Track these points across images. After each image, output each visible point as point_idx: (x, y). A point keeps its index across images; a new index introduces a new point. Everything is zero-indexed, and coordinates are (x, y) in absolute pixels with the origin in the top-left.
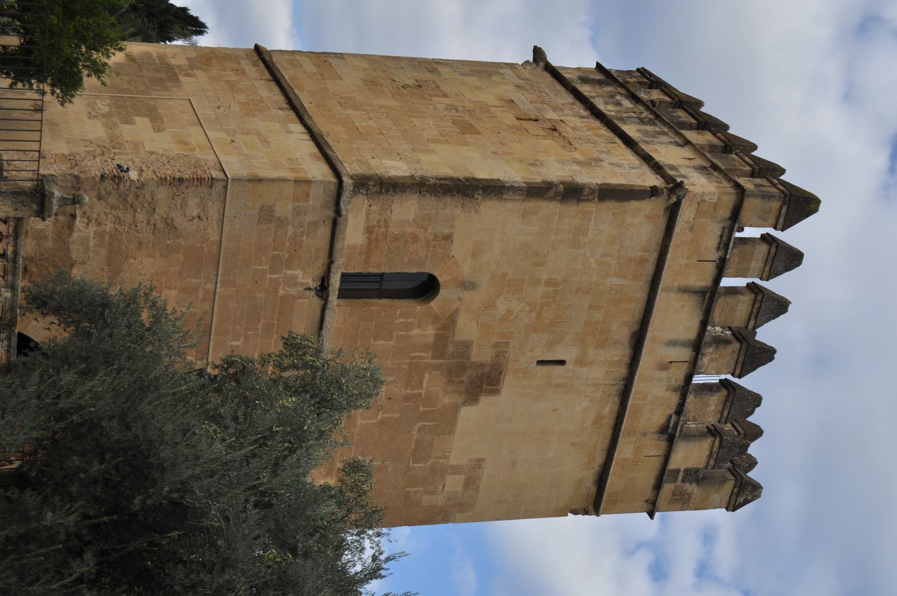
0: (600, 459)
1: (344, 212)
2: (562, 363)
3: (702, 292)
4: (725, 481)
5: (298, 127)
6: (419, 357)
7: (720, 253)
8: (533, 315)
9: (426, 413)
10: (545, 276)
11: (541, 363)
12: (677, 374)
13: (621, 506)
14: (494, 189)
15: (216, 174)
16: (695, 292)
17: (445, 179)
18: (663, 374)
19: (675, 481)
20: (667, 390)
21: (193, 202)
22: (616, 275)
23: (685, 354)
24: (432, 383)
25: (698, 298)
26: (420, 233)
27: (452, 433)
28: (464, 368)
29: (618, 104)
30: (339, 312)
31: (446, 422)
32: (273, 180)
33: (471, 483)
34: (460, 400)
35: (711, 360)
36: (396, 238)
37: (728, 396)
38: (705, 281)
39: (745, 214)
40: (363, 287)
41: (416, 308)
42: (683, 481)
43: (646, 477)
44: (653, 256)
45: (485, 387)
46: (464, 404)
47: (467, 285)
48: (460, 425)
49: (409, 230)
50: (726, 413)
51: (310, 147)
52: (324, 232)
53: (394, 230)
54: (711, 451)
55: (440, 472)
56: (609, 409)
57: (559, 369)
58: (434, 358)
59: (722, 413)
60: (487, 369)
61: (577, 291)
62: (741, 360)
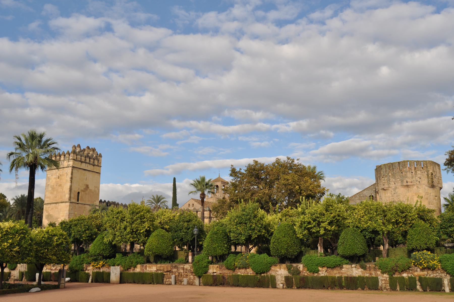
13: (100, 171)
14: (71, 187)
23: (87, 164)
24: (87, 192)
30: (79, 202)
31: (91, 190)
43: (98, 167)
56: (91, 172)
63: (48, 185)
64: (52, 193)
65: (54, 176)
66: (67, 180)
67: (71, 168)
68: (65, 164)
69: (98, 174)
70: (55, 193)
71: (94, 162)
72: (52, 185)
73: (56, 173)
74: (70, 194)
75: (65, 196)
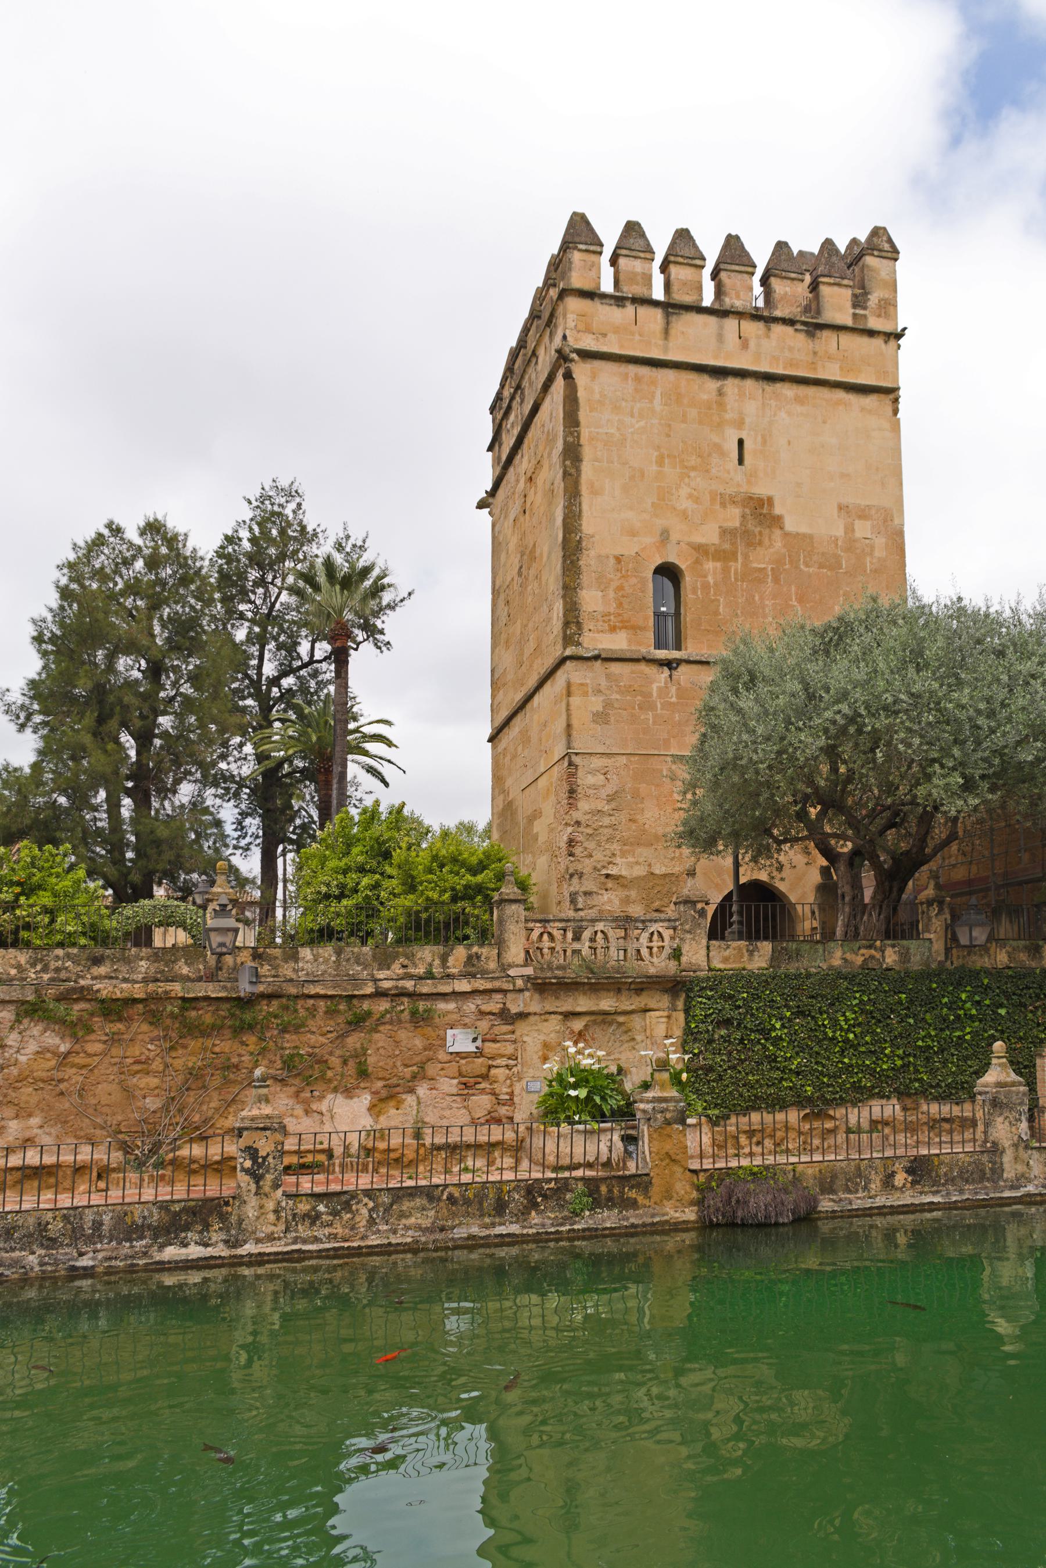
0: (841, 394)
1: (596, 652)
2: (741, 442)
3: (667, 315)
5: (536, 699)
6: (736, 573)
7: (628, 304)
8: (693, 474)
9: (791, 562)
10: (655, 468)
11: (741, 461)
12: (752, 328)
16: (668, 323)
18: (752, 344)
19: (865, 316)
20: (768, 337)
21: (591, 780)
22: (651, 402)
24: (761, 559)
25: (673, 319)
26: (614, 585)
27: (811, 537)
28: (746, 532)
30: (691, 649)
31: (801, 542)
32: (569, 716)
33: (863, 514)
34: (778, 532)
35: (738, 297)
36: (620, 605)
37: (775, 276)
38: (658, 314)
39: (587, 286)
40: (670, 629)
41: (688, 580)
42: (865, 308)
44: (633, 369)
45: (765, 511)
46: (781, 528)
47: (665, 536)
48: (804, 529)
49: (611, 594)
50: (793, 275)
51: (547, 687)
52: (615, 668)
53: (612, 608)
54: (834, 284)
55: (850, 543)
56: (788, 391)
57: (747, 445)
58: (736, 560)
59: (793, 279)
60: (747, 511)
61: (668, 436)
62: (737, 268)
71: (814, 305)
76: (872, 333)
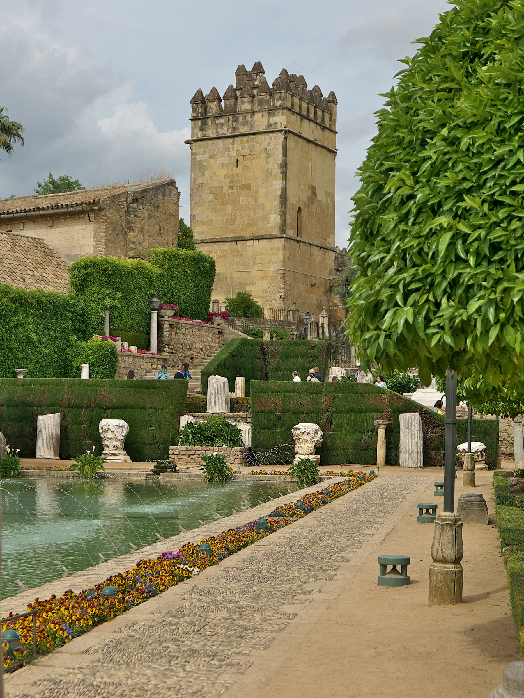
4: (331, 106)
14: (284, 190)
15: (281, 272)
17: (282, 207)
29: (222, 124)
63: (201, 185)
64: (214, 210)
65: (220, 160)
66: (268, 173)
67: (281, 137)
68: (260, 121)
69: (331, 155)
70: (229, 208)
72: (216, 184)
73: (228, 149)
74: (283, 214)
75: (266, 218)
76: (332, 131)
